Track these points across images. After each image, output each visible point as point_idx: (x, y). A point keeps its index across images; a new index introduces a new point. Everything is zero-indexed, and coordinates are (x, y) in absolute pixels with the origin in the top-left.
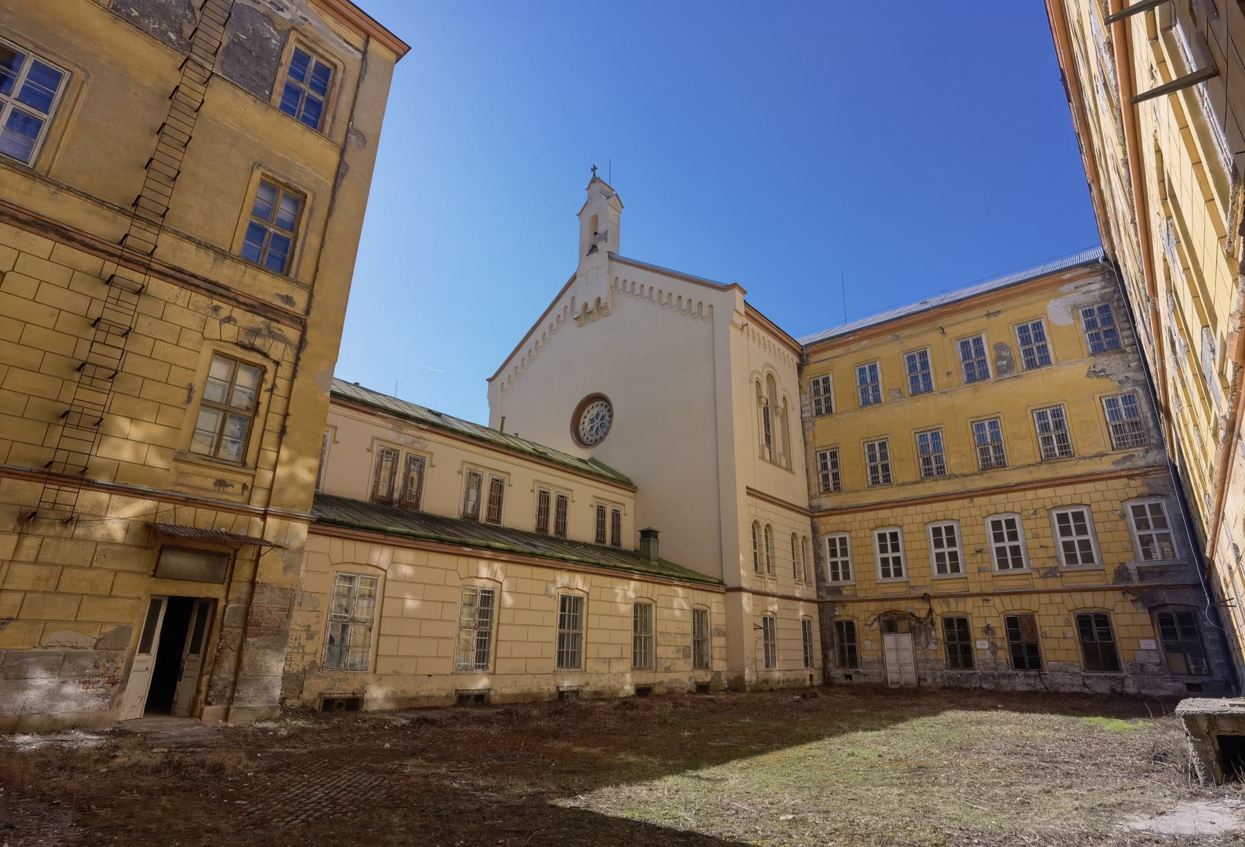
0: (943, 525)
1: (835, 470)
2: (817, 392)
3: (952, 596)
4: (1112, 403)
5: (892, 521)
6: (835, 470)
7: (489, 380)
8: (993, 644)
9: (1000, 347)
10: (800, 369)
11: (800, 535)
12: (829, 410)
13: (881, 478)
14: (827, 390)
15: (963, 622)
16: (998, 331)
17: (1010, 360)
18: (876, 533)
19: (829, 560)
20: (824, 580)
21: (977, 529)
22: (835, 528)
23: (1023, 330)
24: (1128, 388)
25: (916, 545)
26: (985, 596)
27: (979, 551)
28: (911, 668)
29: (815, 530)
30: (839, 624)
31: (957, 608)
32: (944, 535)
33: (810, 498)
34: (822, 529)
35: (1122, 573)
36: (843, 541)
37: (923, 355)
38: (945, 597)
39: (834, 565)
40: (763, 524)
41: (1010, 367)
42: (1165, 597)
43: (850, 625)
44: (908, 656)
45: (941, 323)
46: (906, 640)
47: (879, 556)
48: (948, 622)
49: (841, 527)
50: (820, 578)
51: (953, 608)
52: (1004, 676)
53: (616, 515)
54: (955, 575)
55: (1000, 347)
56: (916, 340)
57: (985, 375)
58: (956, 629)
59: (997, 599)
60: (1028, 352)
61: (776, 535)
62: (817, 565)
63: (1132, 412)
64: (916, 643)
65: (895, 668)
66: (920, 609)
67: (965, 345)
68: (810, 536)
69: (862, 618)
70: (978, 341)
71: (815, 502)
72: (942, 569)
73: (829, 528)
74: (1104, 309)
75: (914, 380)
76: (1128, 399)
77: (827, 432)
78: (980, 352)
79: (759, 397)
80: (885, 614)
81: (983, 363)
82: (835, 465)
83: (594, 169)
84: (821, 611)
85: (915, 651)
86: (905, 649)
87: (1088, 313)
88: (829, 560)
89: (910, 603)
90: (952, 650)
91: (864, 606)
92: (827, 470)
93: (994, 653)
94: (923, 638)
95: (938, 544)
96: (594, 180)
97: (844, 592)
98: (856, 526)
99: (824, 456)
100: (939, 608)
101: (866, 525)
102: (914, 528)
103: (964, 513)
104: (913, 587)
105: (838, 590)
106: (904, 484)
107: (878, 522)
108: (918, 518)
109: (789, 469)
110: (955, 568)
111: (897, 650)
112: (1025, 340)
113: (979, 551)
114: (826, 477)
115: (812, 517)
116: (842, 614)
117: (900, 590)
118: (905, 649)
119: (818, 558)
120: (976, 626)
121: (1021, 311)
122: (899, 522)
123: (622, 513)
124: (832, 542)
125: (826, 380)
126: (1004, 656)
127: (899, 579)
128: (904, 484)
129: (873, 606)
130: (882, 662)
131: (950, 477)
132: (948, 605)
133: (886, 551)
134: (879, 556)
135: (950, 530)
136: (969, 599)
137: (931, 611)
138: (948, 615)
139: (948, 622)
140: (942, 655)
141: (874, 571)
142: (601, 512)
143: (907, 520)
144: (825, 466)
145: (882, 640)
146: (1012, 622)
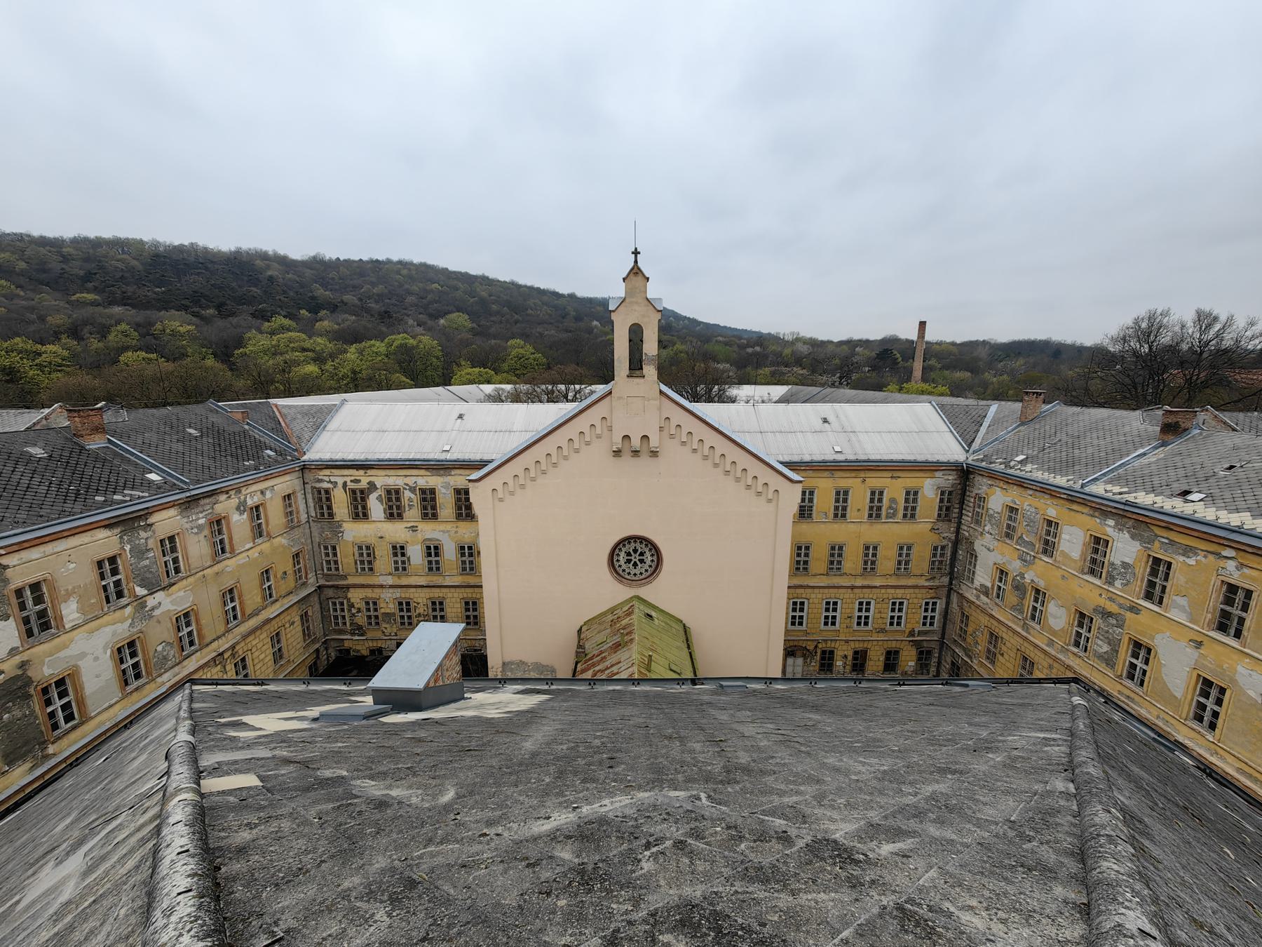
4: (936, 548)
9: (893, 500)
15: (832, 652)
16: (895, 489)
17: (896, 510)
23: (908, 493)
24: (945, 542)
26: (847, 641)
32: (831, 606)
35: (912, 633)
37: (846, 493)
41: (894, 515)
42: (925, 644)
45: (862, 474)
46: (800, 661)
48: (824, 652)
55: (893, 500)
56: (844, 482)
57: (879, 516)
60: (906, 508)
63: (942, 555)
66: (811, 648)
67: (873, 493)
70: (881, 493)
74: (950, 493)
75: (836, 508)
76: (943, 548)
78: (880, 500)
81: (879, 508)
83: (636, 253)
87: (943, 493)
90: (822, 665)
95: (827, 610)
96: (636, 271)
103: (847, 596)
112: (907, 501)
120: (839, 654)
121: (909, 481)
126: (848, 668)
139: (824, 652)
143: (813, 596)
146: (856, 653)
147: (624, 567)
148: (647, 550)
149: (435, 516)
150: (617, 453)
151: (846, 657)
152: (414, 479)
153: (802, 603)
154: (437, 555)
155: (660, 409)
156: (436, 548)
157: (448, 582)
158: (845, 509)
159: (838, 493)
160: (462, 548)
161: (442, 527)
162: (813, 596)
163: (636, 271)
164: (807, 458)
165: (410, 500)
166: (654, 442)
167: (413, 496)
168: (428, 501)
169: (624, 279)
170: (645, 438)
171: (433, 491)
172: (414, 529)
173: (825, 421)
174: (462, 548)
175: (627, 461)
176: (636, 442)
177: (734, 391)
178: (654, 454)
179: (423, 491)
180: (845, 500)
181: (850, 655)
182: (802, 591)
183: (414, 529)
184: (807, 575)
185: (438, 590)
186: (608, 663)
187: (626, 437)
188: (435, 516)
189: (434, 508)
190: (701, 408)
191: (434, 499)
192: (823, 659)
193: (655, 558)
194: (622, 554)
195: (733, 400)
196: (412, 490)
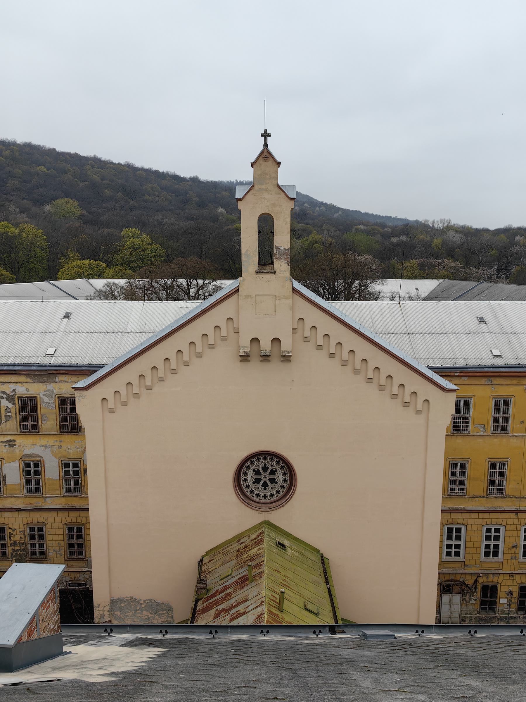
5: (460, 521)
8: (510, 601)
15: (494, 588)
21: (515, 533)
25: (474, 539)
26: (512, 575)
27: (513, 547)
28: (457, 615)
32: (492, 534)
37: (507, 402)
44: (456, 608)
46: (457, 598)
48: (485, 588)
52: (512, 618)
56: (504, 390)
59: (518, 576)
65: (447, 615)
66: (470, 581)
75: (496, 420)
83: (266, 135)
85: (461, 604)
86: (455, 603)
93: (509, 605)
94: (467, 596)
95: (488, 538)
96: (266, 155)
102: (475, 527)
103: (510, 522)
107: (451, 520)
108: (479, 521)
113: (513, 547)
118: (455, 603)
120: (502, 590)
122: (465, 522)
126: (514, 606)
132: (488, 577)
133: (452, 539)
137: (476, 581)
139: (485, 588)
140: (478, 606)
143: (471, 521)
147: (252, 487)
148: (278, 468)
149: (35, 429)
150: (245, 358)
151: (510, 593)
152: (12, 387)
153: (459, 530)
154: (37, 473)
155: (292, 309)
156: (36, 465)
157: (49, 504)
158: (505, 420)
159: (497, 403)
160: (67, 465)
161: (44, 441)
162: (471, 521)
163: (266, 155)
164: (461, 363)
165: (7, 410)
166: (286, 346)
167: (10, 406)
168: (28, 409)
169: (253, 164)
170: (276, 341)
171: (34, 400)
172: (11, 443)
173: (481, 320)
174: (67, 465)
175: (255, 367)
176: (266, 345)
177: (377, 287)
178: (286, 359)
179: (22, 400)
180: (506, 411)
181: (516, 590)
182: (458, 515)
183: (11, 443)
184: (464, 497)
185: (37, 514)
186: (233, 601)
187: (255, 340)
188: (35, 429)
189: (35, 419)
190: (338, 307)
191: (35, 410)
192: (484, 595)
193: (288, 478)
194: (250, 473)
195: (375, 297)
196: (10, 398)
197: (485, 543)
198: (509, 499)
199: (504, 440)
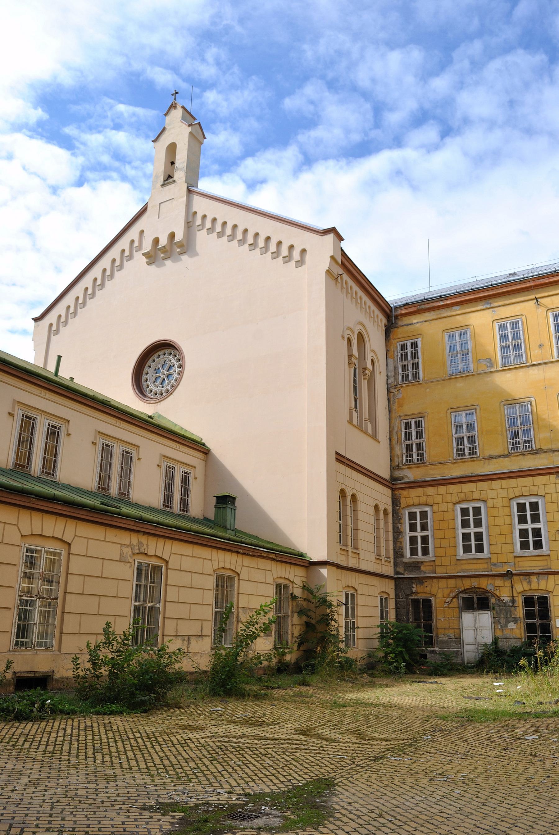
0: (527, 501)
1: (419, 441)
2: (404, 357)
3: (533, 574)
5: (476, 496)
6: (419, 441)
7: (36, 320)
10: (388, 331)
11: (382, 508)
12: (416, 376)
13: (467, 451)
14: (415, 355)
18: (458, 507)
19: (408, 534)
20: (402, 556)
22: (416, 501)
29: (395, 502)
30: (416, 602)
31: (538, 586)
33: (394, 468)
34: (403, 503)
36: (424, 515)
38: (527, 575)
39: (413, 540)
40: (349, 493)
43: (428, 603)
47: (461, 531)
48: (528, 601)
49: (423, 500)
50: (398, 553)
51: (534, 586)
53: (185, 479)
54: (538, 552)
58: (537, 608)
61: (361, 506)
62: (395, 540)
64: (495, 622)
68: (390, 509)
69: (440, 595)
71: (398, 474)
72: (524, 546)
73: (410, 502)
77: (413, 401)
79: (350, 356)
80: (464, 591)
82: (419, 435)
84: (397, 588)
85: (494, 628)
88: (408, 534)
89: (490, 581)
91: (443, 583)
92: (409, 437)
95: (522, 520)
97: (423, 568)
98: (438, 499)
99: (408, 425)
100: (520, 586)
101: (448, 498)
103: (550, 489)
104: (494, 564)
105: (416, 566)
106: (491, 458)
107: (462, 496)
109: (374, 436)
110: (538, 545)
111: (475, 629)
114: (409, 448)
115: (393, 490)
116: (421, 591)
117: (481, 568)
119: (397, 533)
122: (483, 497)
123: (192, 477)
124: (412, 516)
125: (414, 345)
127: (480, 555)
128: (491, 458)
129: (452, 582)
130: (459, 640)
131: (537, 452)
132: (530, 582)
134: (461, 531)
135: (534, 506)
136: (551, 577)
138: (529, 594)
139: (528, 601)
141: (455, 547)
142: (170, 473)
144: (408, 436)
145: (460, 618)
153: (477, 511)
184: (476, 459)
192: (529, 615)
197: (518, 527)
198: (543, 455)
199: (521, 373)
